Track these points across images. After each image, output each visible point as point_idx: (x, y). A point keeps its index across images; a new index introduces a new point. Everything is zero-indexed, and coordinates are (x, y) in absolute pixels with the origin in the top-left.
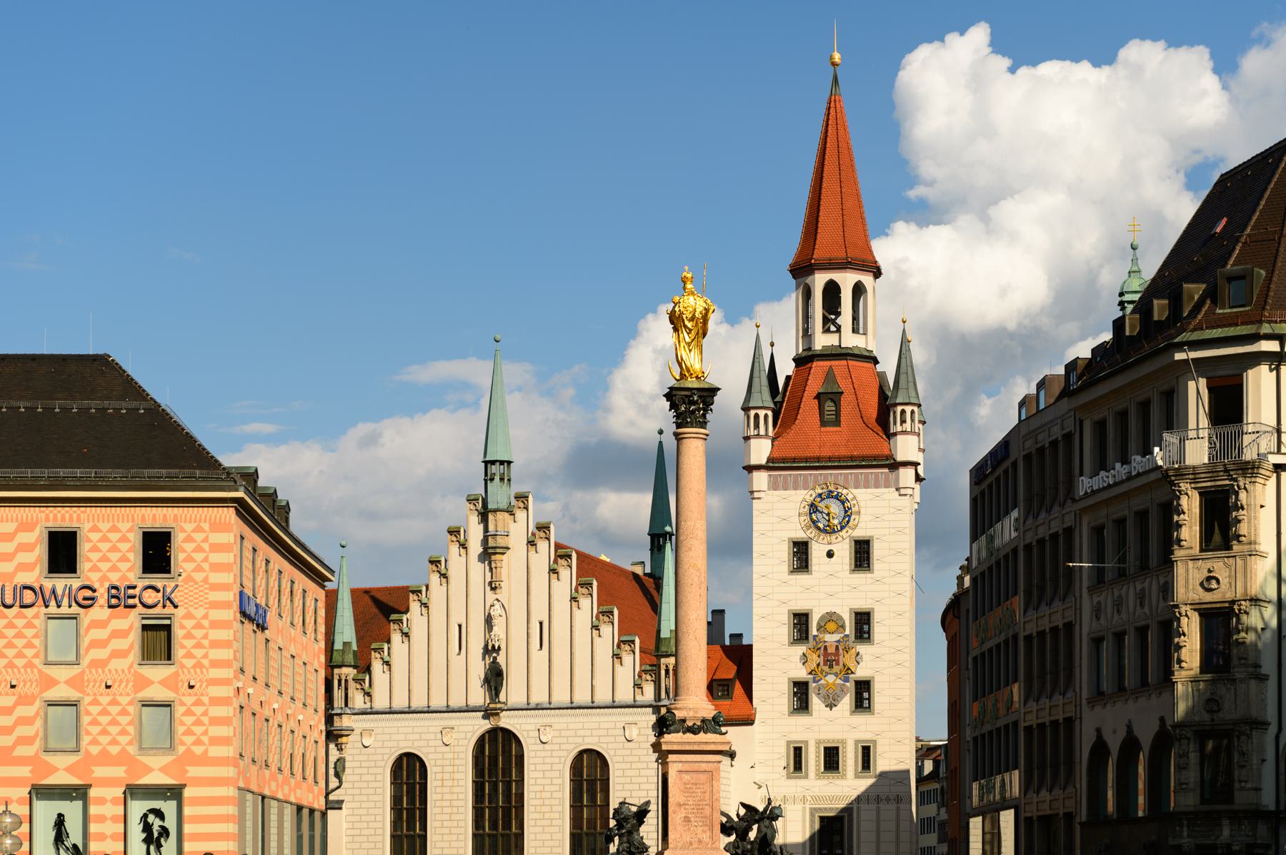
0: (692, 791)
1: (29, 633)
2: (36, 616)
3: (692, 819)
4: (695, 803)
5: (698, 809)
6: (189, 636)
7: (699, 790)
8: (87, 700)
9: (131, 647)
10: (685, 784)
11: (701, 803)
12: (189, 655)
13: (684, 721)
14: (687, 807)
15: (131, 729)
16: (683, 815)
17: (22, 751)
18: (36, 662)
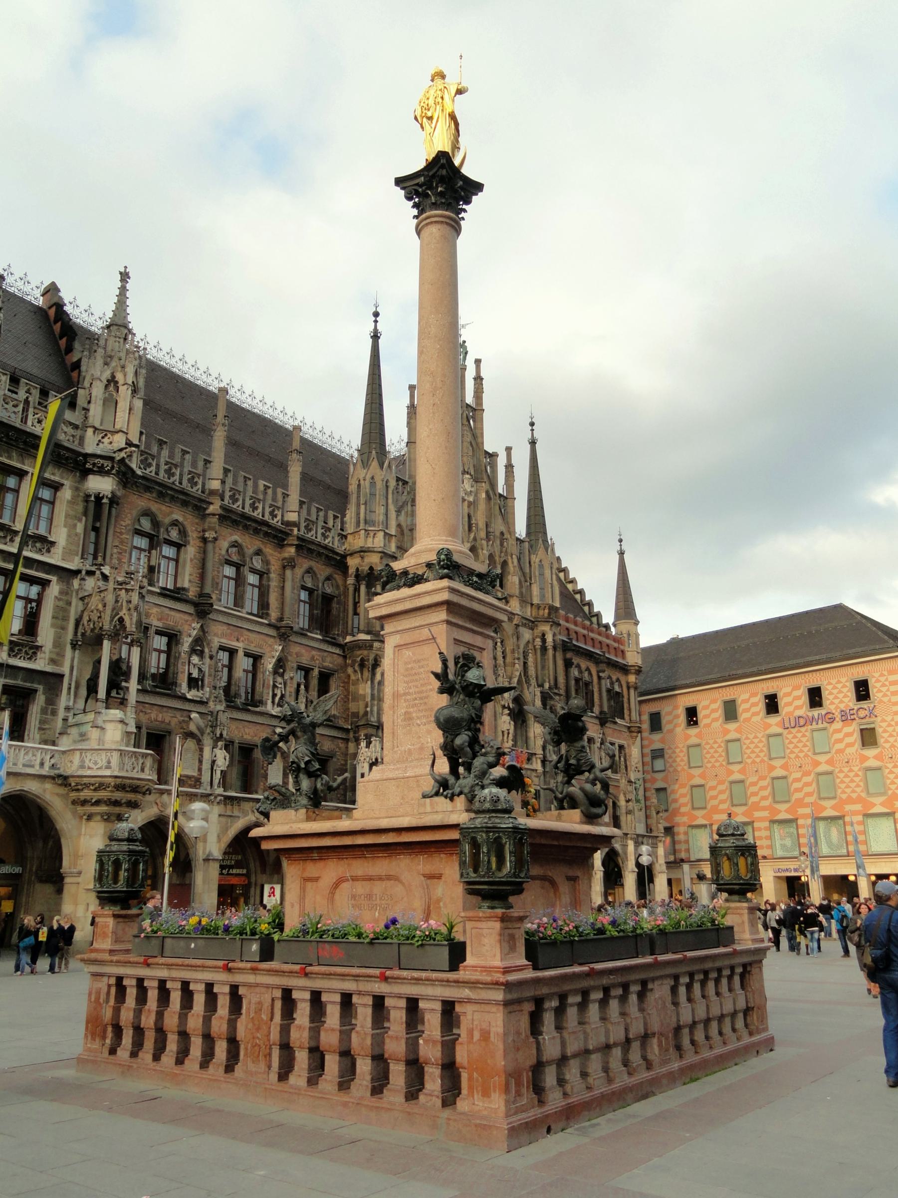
0: (414, 671)
1: (804, 739)
2: (806, 731)
3: (414, 715)
4: (417, 690)
5: (421, 698)
6: (885, 731)
7: (422, 670)
8: (837, 770)
9: (855, 741)
10: (406, 663)
11: (424, 689)
12: (887, 741)
13: (405, 573)
14: (408, 697)
15: (862, 784)
16: (403, 711)
17: (808, 800)
18: (810, 754)
